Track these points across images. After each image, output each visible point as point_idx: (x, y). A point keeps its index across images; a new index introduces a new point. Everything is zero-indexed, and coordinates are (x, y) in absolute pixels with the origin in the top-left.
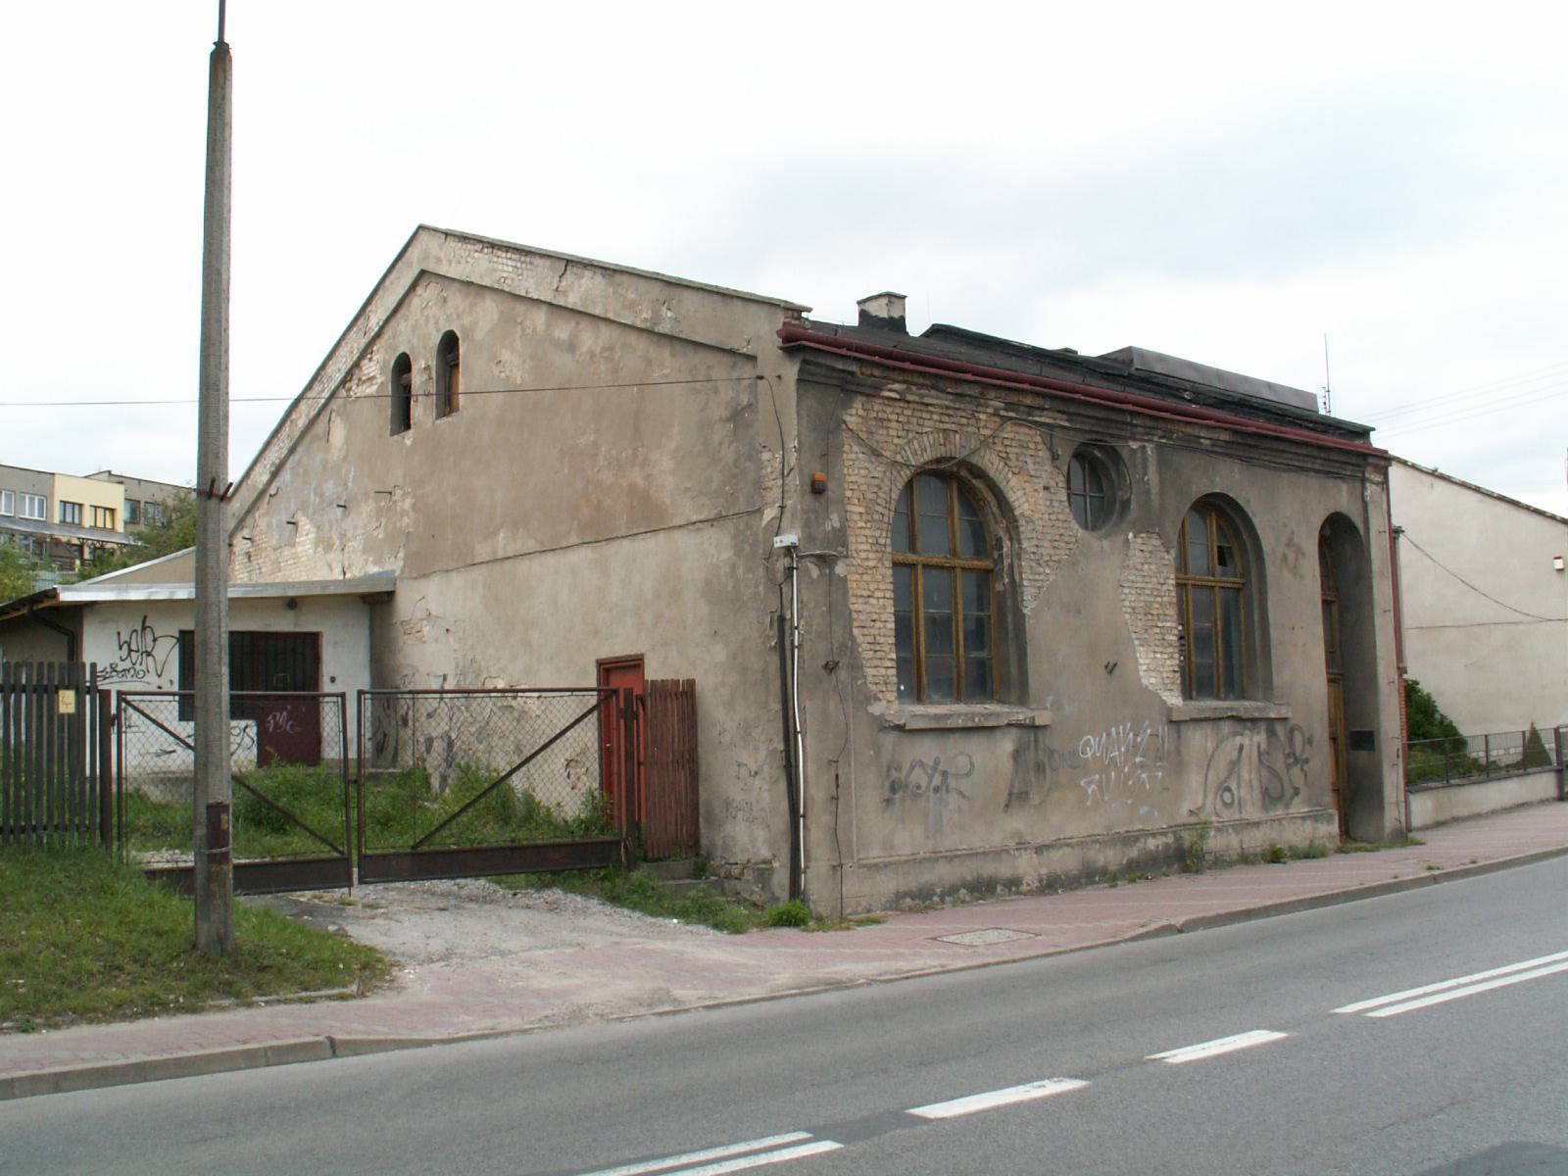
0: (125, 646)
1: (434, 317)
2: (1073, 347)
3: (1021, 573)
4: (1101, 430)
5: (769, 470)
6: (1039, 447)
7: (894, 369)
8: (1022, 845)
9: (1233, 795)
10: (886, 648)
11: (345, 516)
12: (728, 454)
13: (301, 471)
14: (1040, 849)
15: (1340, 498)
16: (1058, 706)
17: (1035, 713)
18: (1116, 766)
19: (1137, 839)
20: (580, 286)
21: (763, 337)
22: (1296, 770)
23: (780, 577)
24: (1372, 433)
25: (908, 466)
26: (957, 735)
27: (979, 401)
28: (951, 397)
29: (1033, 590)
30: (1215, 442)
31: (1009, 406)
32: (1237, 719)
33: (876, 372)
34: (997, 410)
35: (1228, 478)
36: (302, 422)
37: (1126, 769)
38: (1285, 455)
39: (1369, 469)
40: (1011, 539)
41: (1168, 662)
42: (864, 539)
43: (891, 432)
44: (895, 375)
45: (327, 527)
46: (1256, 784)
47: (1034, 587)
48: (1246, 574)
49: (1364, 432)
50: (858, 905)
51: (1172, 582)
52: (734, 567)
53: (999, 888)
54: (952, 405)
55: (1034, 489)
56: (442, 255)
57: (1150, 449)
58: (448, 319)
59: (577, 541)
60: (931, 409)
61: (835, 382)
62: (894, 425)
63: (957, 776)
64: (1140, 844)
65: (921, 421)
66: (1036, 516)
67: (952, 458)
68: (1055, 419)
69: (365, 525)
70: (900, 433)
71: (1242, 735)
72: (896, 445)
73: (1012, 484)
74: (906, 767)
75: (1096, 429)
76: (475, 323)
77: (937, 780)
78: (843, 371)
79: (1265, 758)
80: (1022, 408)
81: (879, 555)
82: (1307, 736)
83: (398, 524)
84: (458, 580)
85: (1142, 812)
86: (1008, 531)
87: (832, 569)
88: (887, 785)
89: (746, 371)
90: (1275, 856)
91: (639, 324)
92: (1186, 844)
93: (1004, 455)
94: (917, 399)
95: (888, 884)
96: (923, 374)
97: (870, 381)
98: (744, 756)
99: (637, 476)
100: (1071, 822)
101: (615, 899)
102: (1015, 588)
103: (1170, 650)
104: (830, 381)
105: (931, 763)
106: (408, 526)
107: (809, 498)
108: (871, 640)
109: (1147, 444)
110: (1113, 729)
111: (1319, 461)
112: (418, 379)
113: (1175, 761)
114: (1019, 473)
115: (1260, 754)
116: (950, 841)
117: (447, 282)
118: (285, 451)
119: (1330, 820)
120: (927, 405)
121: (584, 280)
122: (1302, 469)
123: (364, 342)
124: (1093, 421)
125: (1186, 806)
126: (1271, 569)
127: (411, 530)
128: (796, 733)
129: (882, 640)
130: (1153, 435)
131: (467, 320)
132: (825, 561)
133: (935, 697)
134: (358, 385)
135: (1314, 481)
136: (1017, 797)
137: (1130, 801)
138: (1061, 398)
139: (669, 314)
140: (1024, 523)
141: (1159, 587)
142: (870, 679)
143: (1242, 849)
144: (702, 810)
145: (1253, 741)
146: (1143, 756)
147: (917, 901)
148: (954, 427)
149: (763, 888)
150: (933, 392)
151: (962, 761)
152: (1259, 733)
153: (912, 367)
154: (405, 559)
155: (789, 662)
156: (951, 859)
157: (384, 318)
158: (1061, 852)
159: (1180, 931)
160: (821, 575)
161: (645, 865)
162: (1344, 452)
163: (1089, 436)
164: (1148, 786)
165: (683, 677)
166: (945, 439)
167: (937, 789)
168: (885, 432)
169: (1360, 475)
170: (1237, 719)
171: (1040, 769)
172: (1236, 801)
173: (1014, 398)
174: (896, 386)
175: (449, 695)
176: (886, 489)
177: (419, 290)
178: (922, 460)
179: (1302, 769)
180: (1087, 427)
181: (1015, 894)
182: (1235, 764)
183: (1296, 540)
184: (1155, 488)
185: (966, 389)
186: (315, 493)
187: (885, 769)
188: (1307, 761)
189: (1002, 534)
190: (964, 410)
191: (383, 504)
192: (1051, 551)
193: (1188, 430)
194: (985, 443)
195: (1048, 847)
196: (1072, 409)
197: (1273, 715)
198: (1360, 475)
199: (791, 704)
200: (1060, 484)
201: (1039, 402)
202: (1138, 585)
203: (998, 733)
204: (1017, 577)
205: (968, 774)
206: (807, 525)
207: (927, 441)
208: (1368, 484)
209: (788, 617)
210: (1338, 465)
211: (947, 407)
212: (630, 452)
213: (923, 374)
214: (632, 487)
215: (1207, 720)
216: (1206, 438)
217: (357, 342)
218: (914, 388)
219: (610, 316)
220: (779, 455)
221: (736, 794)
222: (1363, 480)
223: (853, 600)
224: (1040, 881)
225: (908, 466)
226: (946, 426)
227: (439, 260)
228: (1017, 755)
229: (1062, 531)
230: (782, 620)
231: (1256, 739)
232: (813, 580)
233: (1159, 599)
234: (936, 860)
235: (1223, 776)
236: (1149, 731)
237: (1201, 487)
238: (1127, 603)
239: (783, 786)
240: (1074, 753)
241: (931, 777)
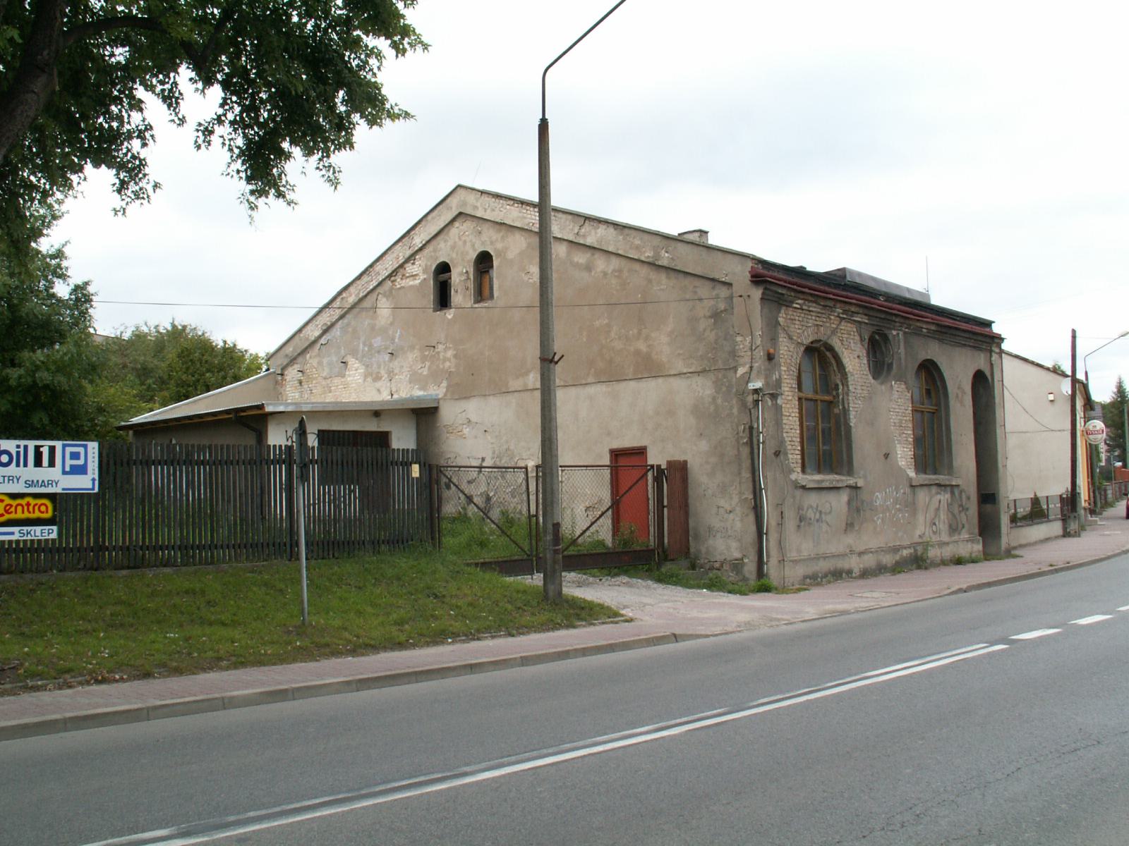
0: (290, 439)
1: (471, 241)
2: (804, 265)
3: (849, 403)
5: (741, 346)
8: (852, 552)
11: (391, 360)
12: (711, 336)
13: (350, 330)
14: (861, 554)
15: (980, 361)
16: (865, 477)
19: (898, 550)
20: (596, 233)
21: (741, 275)
22: (963, 514)
23: (750, 404)
24: (993, 325)
26: (825, 491)
27: (832, 308)
31: (845, 312)
32: (939, 485)
33: (793, 294)
34: (839, 314)
35: (934, 351)
36: (352, 299)
39: (995, 345)
40: (843, 385)
43: (797, 326)
45: (375, 366)
46: (946, 521)
48: (938, 404)
49: (988, 324)
51: (910, 409)
52: (714, 399)
53: (844, 575)
56: (479, 204)
57: (901, 333)
58: (483, 243)
59: (593, 381)
62: (797, 322)
63: (826, 514)
67: (820, 340)
69: (411, 367)
70: (802, 325)
74: (805, 508)
76: (507, 249)
83: (441, 366)
84: (493, 401)
86: (842, 381)
89: (724, 292)
90: (959, 561)
91: (643, 258)
92: (919, 553)
95: (800, 571)
98: (722, 503)
99: (642, 346)
100: (875, 538)
101: (660, 580)
102: (846, 412)
103: (910, 446)
105: (815, 506)
106: (450, 367)
107: (767, 363)
112: (456, 277)
117: (481, 221)
118: (336, 317)
120: (810, 311)
121: (600, 230)
122: (965, 345)
123: (408, 253)
125: (918, 532)
126: (952, 402)
127: (453, 370)
128: (761, 490)
129: (794, 439)
131: (499, 246)
132: (774, 396)
134: (402, 279)
136: (849, 526)
138: (867, 309)
139: (666, 255)
144: (691, 533)
145: (945, 497)
148: (821, 323)
149: (737, 574)
150: (814, 305)
151: (828, 505)
154: (448, 388)
155: (756, 451)
156: (825, 558)
157: (427, 239)
159: (965, 592)
160: (772, 404)
161: (668, 563)
162: (976, 334)
165: (682, 458)
167: (818, 521)
170: (939, 485)
171: (858, 510)
174: (800, 301)
175: (487, 470)
177: (456, 224)
182: (938, 509)
184: (903, 356)
186: (364, 344)
188: (967, 509)
189: (839, 382)
191: (427, 353)
192: (861, 391)
193: (918, 324)
196: (871, 313)
197: (954, 483)
199: (757, 473)
203: (841, 491)
204: (846, 406)
206: (767, 377)
207: (810, 331)
208: (993, 354)
209: (755, 426)
211: (819, 313)
212: (635, 331)
213: (811, 295)
214: (638, 353)
215: (926, 485)
217: (402, 253)
219: (620, 252)
220: (749, 339)
221: (716, 523)
222: (991, 351)
225: (803, 345)
226: (818, 323)
227: (476, 208)
228: (849, 503)
230: (751, 428)
234: (818, 559)
235: (933, 517)
237: (923, 355)
239: (751, 518)
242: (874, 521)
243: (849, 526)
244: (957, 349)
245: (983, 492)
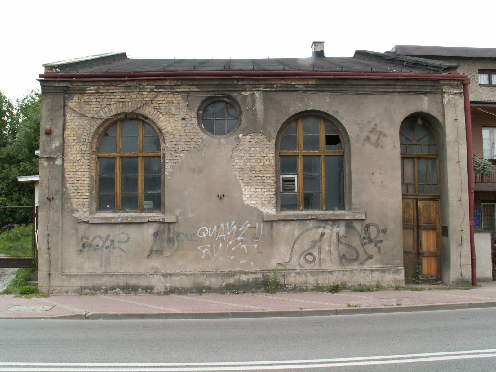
4: (220, 89)
6: (180, 102)
7: (88, 82)
8: (157, 273)
10: (84, 191)
14: (165, 275)
17: (166, 217)
18: (223, 241)
19: (234, 275)
25: (101, 119)
26: (121, 226)
28: (123, 88)
29: (171, 164)
30: (307, 86)
31: (157, 87)
33: (79, 84)
37: (231, 243)
38: (370, 87)
41: (266, 193)
42: (75, 149)
44: (89, 84)
46: (335, 252)
47: (173, 163)
50: (61, 290)
53: (140, 290)
54: (125, 91)
55: (175, 119)
60: (115, 94)
61: (59, 91)
62: (94, 103)
63: (120, 242)
64: (237, 277)
65: (110, 100)
66: (176, 131)
68: (189, 89)
72: (95, 111)
73: (161, 119)
74: (91, 238)
75: (217, 89)
77: (108, 243)
78: (59, 86)
79: (343, 240)
80: (166, 87)
81: (83, 155)
82: (381, 229)
85: (241, 262)
87: (54, 163)
88: (81, 245)
93: (157, 108)
94: (105, 91)
95: (77, 283)
96: (104, 81)
97: (78, 88)
100: (183, 265)
103: (269, 187)
104: (57, 91)
105: (105, 236)
108: (76, 188)
109: (255, 92)
110: (222, 225)
111: (398, 87)
113: (271, 241)
114: (166, 114)
116: (112, 269)
119: (397, 272)
120: (113, 93)
124: (214, 86)
130: (259, 88)
133: (128, 210)
135: (397, 98)
137: (232, 257)
140: (168, 135)
141: (263, 158)
142: (74, 203)
143: (317, 284)
146: (243, 236)
147: (92, 291)
148: (128, 100)
150: (112, 87)
153: (129, 78)
158: (179, 278)
160: (49, 165)
163: (213, 93)
164: (246, 251)
166: (123, 105)
167: (108, 247)
168: (89, 106)
169: (439, 91)
171: (170, 241)
173: (157, 83)
174: (92, 88)
176: (88, 129)
178: (110, 115)
179: (376, 245)
180: (211, 89)
181: (149, 293)
182: (316, 243)
183: (379, 129)
185: (128, 84)
187: (80, 238)
188: (381, 241)
190: (134, 92)
194: (146, 104)
195: (171, 275)
196: (195, 83)
197: (347, 218)
198: (439, 91)
200: (193, 117)
201: (175, 82)
202: (246, 158)
205: (126, 242)
207: (112, 107)
208: (446, 95)
210: (417, 87)
211: (124, 92)
213: (104, 81)
216: (299, 84)
218: (101, 87)
222: (442, 93)
223: (69, 173)
224: (166, 289)
225: (101, 119)
226: (123, 100)
228: (156, 235)
229: (192, 137)
231: (336, 230)
232: (44, 167)
233: (262, 164)
234: (103, 275)
235: (306, 247)
236: (249, 225)
238: (237, 167)
240: (195, 234)
241: (105, 242)
242: (196, 249)
244: (370, 97)
245: (443, 225)
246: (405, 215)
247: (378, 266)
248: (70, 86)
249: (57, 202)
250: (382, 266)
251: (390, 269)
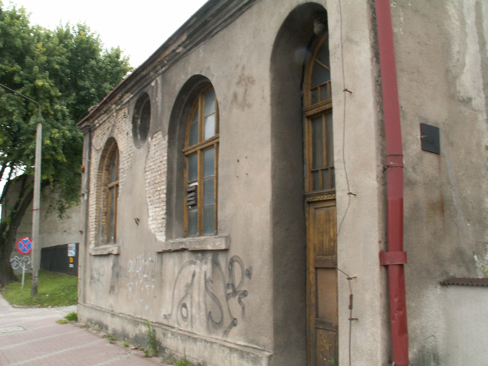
9: (187, 311)
22: (234, 301)
46: (203, 306)
68: (128, 97)
71: (195, 263)
82: (246, 267)
115: (206, 282)
124: (136, 87)
137: (142, 300)
145: (204, 268)
146: (147, 274)
152: (206, 263)
172: (189, 316)
174: (96, 121)
179: (240, 301)
188: (245, 294)
243: (112, 288)
246: (324, 238)
247: (243, 343)
248: (89, 124)
249: (84, 234)
250: (246, 344)
251: (248, 353)
